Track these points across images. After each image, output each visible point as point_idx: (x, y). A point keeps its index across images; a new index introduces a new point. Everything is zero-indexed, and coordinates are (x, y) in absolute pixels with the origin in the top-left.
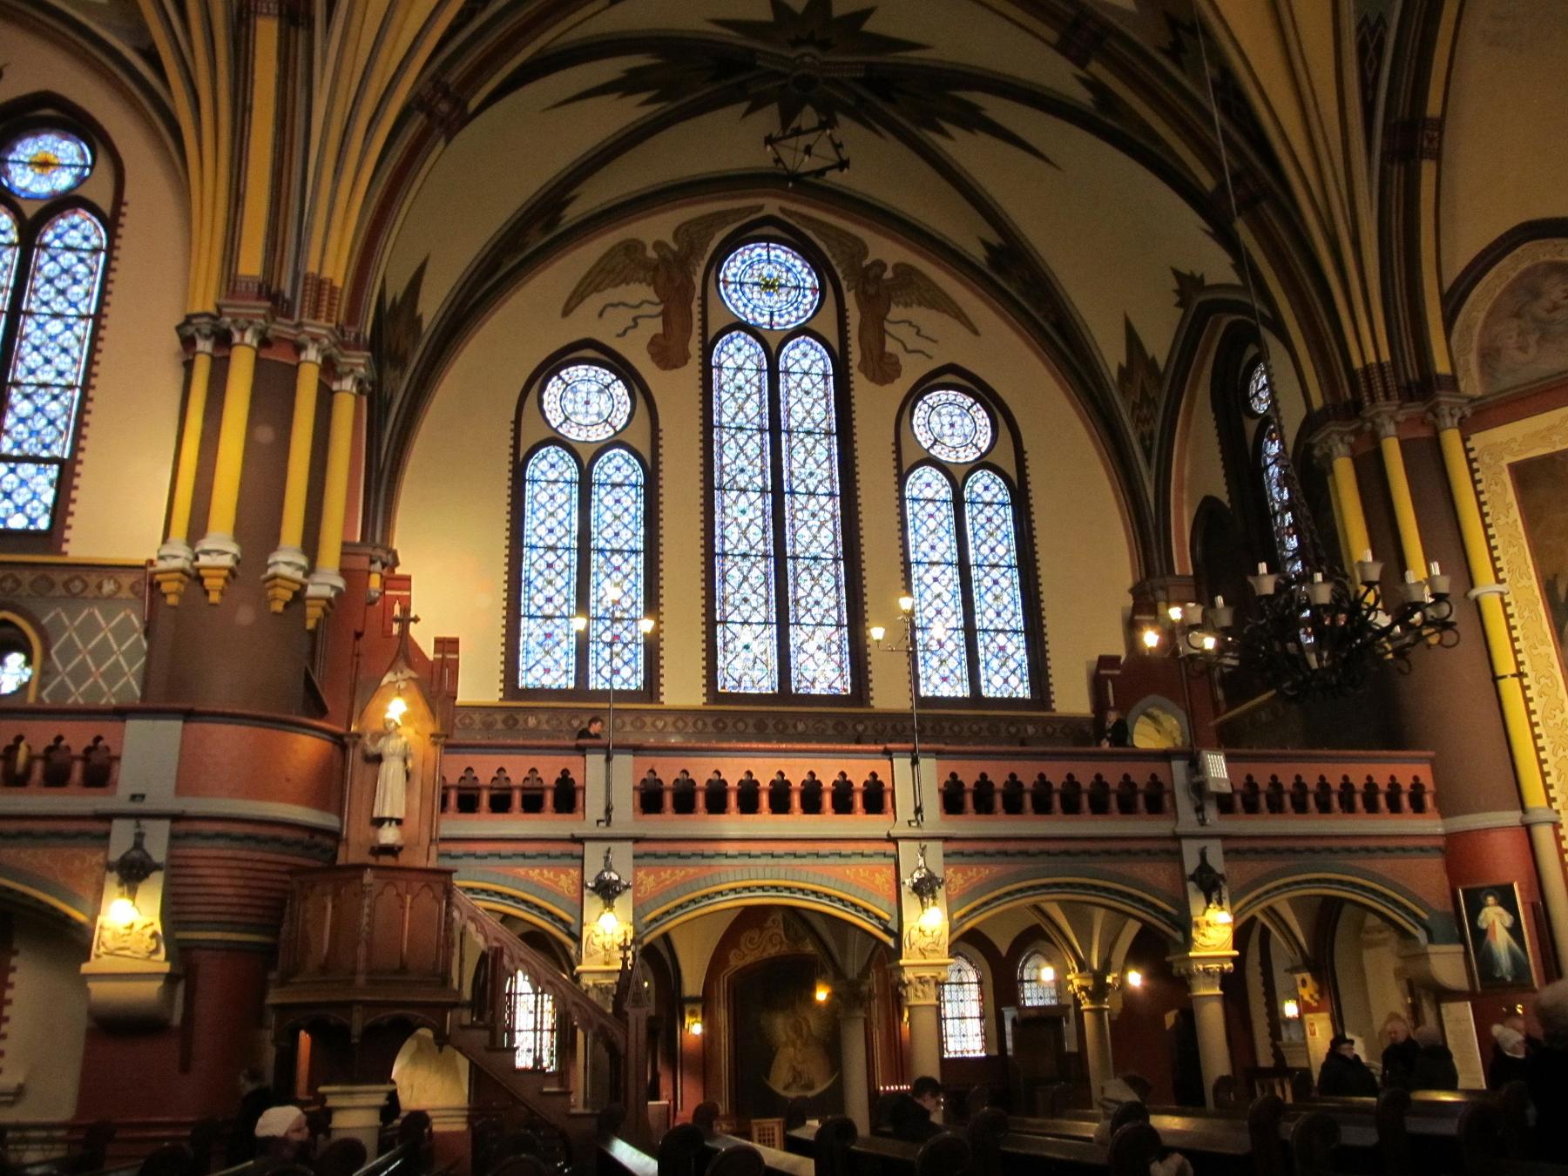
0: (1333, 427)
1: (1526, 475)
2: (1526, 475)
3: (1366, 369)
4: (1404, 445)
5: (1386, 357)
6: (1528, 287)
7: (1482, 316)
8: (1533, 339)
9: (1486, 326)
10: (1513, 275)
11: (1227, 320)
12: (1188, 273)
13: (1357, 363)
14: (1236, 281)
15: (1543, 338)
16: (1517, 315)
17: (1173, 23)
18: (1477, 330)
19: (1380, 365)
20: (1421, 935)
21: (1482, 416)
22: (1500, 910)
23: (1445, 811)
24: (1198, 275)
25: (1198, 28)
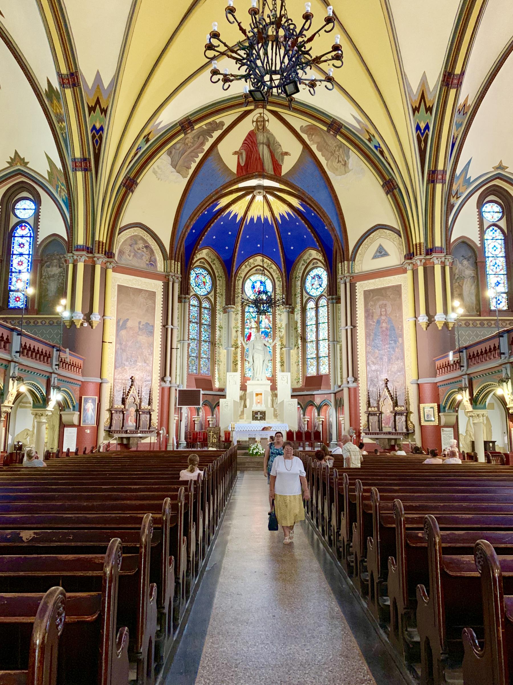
0: (84, 253)
1: (121, 289)
2: (121, 289)
3: (99, 242)
4: (101, 268)
5: (104, 241)
6: (134, 239)
7: (123, 240)
8: (132, 254)
9: (123, 243)
10: (133, 234)
11: (24, 179)
12: (22, 157)
13: (97, 239)
14: (46, 176)
15: (135, 256)
16: (131, 246)
17: (98, 102)
18: (120, 244)
19: (103, 243)
20: (71, 407)
21: (118, 269)
22: (92, 404)
23: (83, 376)
24: (26, 161)
25: (104, 111)
